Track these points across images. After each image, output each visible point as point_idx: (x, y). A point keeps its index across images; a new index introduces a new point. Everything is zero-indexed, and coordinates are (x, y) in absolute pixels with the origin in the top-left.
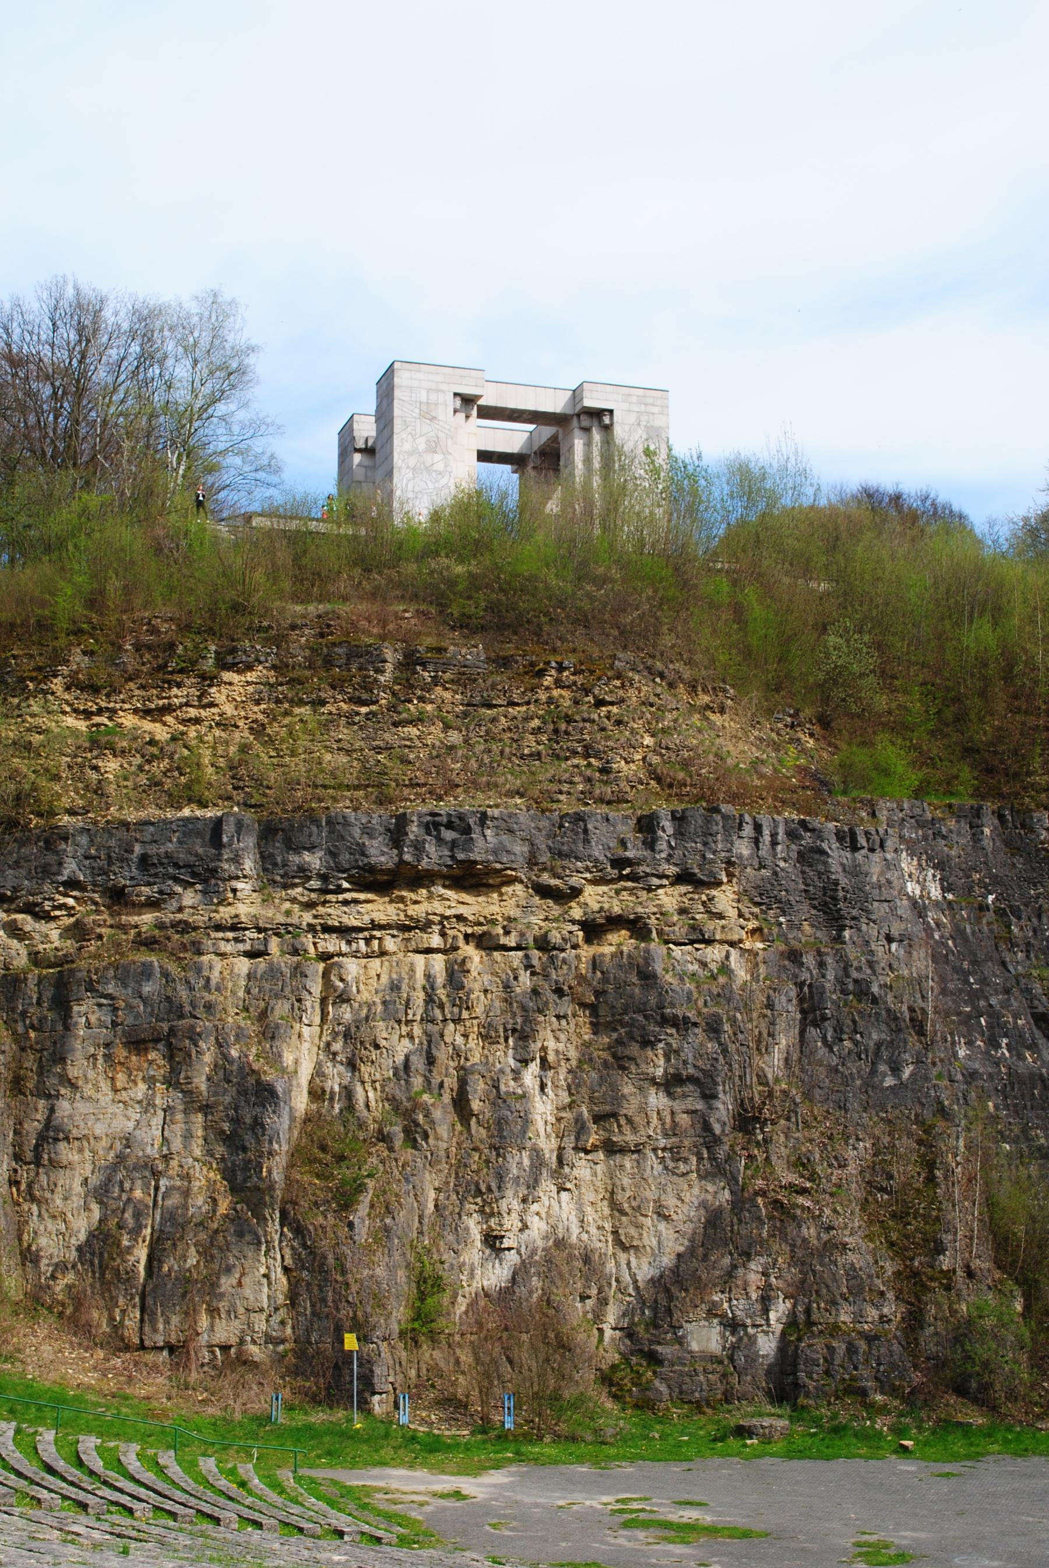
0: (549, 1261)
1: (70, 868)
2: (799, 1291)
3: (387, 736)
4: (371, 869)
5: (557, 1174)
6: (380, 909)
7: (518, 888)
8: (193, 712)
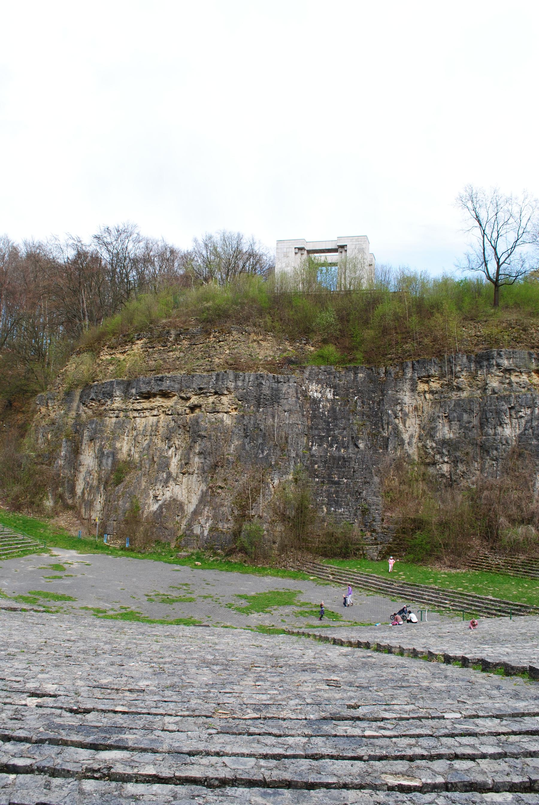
0: (170, 504)
1: (93, 395)
2: (215, 517)
3: (165, 356)
4: (142, 393)
5: (175, 480)
6: (146, 404)
7: (175, 398)
8: (129, 352)
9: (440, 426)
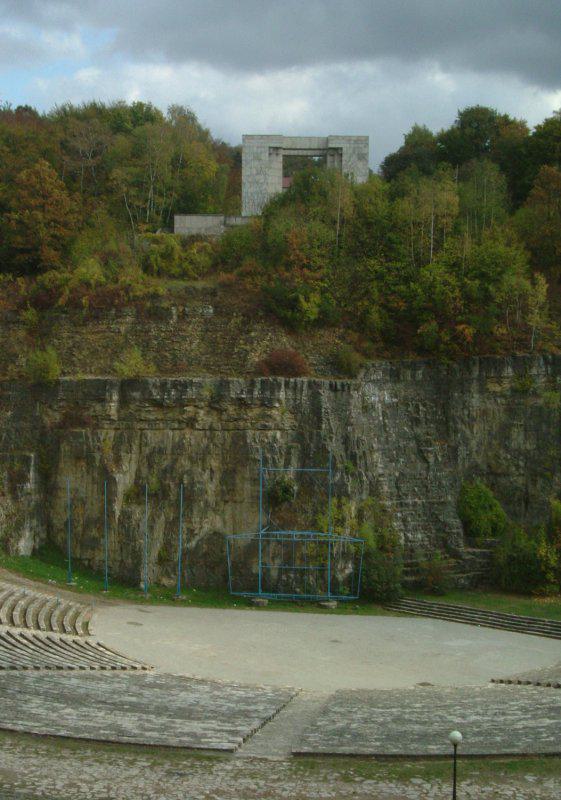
9: (514, 435)
